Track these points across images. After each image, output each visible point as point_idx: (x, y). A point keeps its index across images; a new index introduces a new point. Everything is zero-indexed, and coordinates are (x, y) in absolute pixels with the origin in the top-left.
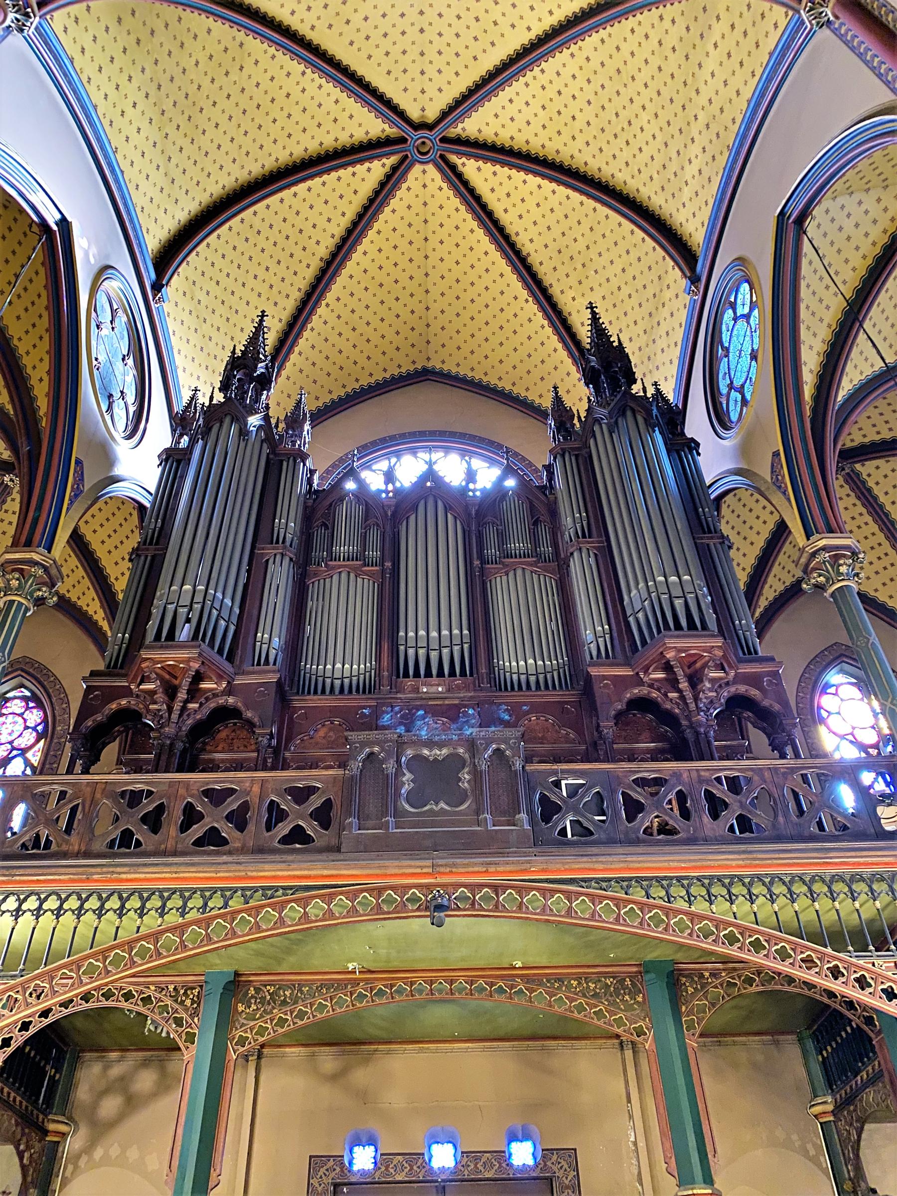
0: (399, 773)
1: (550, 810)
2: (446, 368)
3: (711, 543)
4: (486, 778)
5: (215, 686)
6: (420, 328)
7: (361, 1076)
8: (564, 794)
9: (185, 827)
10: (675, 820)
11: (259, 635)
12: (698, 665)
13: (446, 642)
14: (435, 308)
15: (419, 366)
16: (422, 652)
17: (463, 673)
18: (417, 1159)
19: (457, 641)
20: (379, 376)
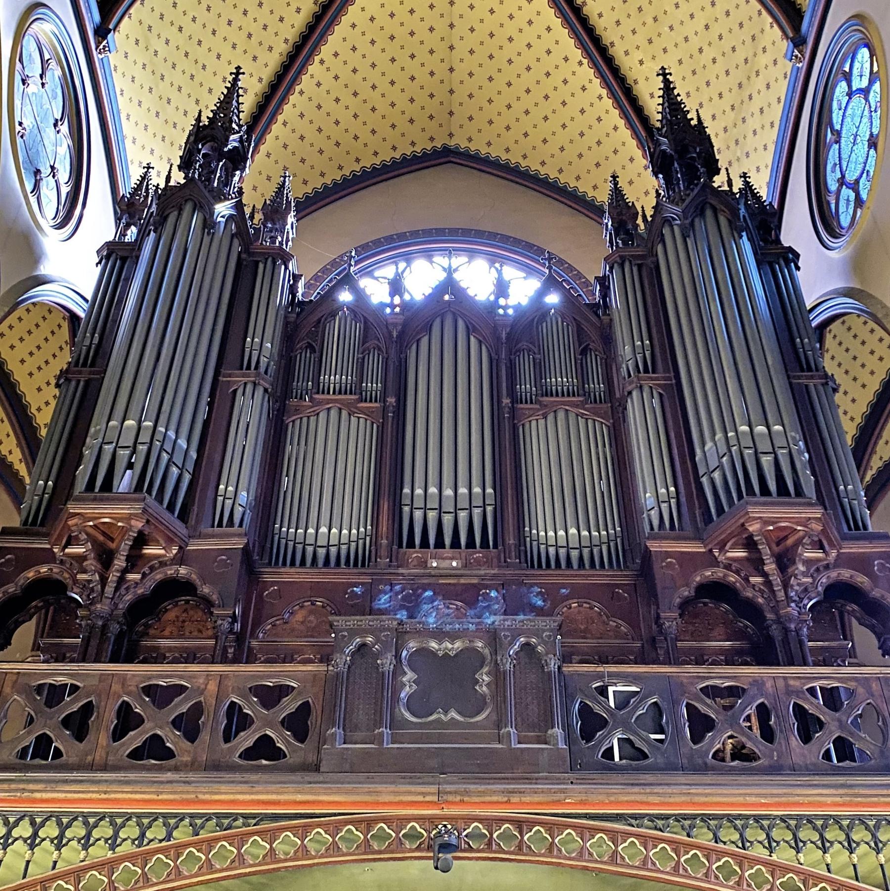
0: (398, 671)
2: (473, 147)
3: (811, 383)
4: (511, 681)
5: (162, 552)
6: (441, 94)
8: (612, 704)
9: (118, 734)
10: (754, 742)
11: (222, 487)
12: (790, 541)
13: (463, 503)
16: (432, 515)
17: (485, 544)
19: (477, 502)
20: (386, 156)
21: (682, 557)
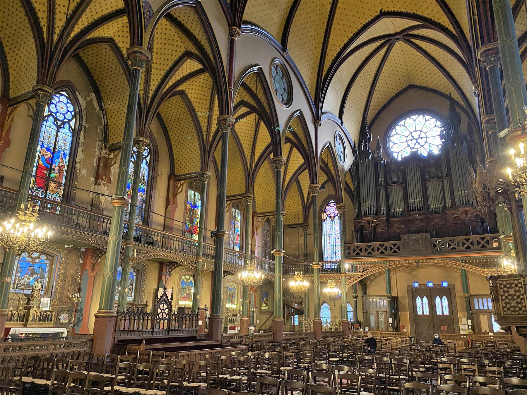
1: (435, 246)
2: (416, 84)
9: (378, 251)
13: (418, 202)
14: (410, 70)
15: (407, 85)
16: (413, 205)
21: (452, 213)
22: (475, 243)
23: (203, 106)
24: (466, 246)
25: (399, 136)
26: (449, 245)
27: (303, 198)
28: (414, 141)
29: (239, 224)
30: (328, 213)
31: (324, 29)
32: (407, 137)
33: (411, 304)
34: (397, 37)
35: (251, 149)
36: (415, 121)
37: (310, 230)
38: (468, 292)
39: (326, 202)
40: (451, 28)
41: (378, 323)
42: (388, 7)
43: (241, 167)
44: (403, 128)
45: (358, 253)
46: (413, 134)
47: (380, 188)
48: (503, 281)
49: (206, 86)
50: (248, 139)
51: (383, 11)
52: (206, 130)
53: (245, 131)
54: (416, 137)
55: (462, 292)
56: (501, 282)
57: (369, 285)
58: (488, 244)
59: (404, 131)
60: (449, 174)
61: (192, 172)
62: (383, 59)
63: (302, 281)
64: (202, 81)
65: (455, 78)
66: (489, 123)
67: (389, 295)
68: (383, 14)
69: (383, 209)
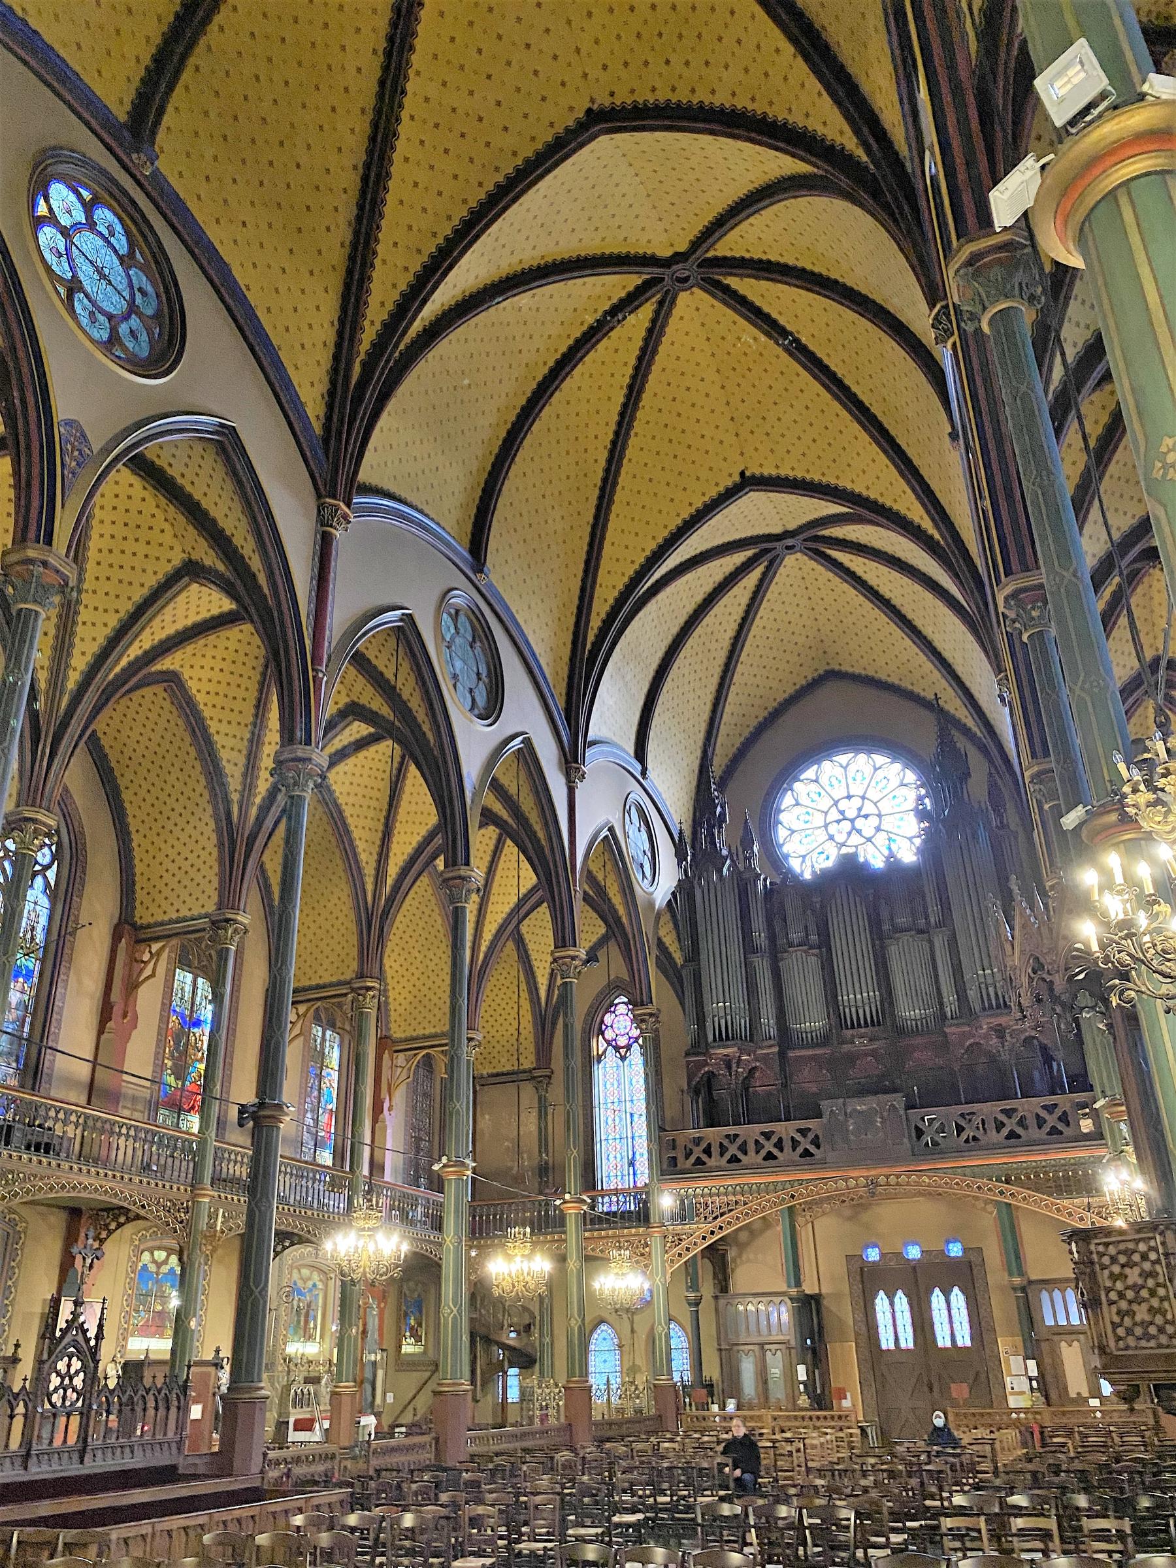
1: (920, 1133)
7: (866, 1217)
9: (757, 1152)
15: (821, 672)
18: (899, 1255)
22: (1031, 1121)
23: (235, 717)
24: (1005, 1131)
25: (804, 810)
26: (960, 1129)
27: (537, 989)
28: (846, 825)
29: (335, 1075)
30: (609, 1035)
31: (589, 516)
32: (826, 813)
33: (860, 1316)
34: (790, 542)
35: (378, 842)
36: (845, 768)
37: (556, 1093)
38: (1021, 1273)
39: (603, 1004)
40: (927, 525)
41: (765, 1382)
42: (761, 465)
43: (344, 898)
44: (813, 787)
45: (699, 1162)
46: (842, 805)
47: (756, 959)
48: (1107, 1245)
49: (246, 659)
50: (371, 813)
51: (748, 474)
52: (239, 788)
53: (361, 791)
54: (851, 814)
55: (1006, 1274)
56: (1101, 1248)
57: (734, 1260)
58: (1068, 1124)
59: (815, 797)
60: (946, 920)
61: (189, 914)
62: (753, 599)
63: (529, 1257)
64: (232, 645)
65: (946, 655)
66: (1041, 782)
67: (793, 1291)
68: (748, 483)
69: (768, 1023)
